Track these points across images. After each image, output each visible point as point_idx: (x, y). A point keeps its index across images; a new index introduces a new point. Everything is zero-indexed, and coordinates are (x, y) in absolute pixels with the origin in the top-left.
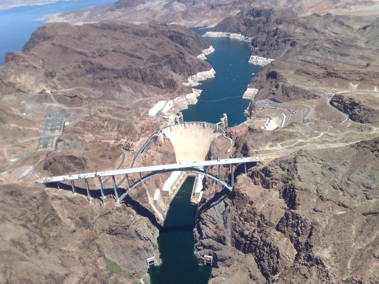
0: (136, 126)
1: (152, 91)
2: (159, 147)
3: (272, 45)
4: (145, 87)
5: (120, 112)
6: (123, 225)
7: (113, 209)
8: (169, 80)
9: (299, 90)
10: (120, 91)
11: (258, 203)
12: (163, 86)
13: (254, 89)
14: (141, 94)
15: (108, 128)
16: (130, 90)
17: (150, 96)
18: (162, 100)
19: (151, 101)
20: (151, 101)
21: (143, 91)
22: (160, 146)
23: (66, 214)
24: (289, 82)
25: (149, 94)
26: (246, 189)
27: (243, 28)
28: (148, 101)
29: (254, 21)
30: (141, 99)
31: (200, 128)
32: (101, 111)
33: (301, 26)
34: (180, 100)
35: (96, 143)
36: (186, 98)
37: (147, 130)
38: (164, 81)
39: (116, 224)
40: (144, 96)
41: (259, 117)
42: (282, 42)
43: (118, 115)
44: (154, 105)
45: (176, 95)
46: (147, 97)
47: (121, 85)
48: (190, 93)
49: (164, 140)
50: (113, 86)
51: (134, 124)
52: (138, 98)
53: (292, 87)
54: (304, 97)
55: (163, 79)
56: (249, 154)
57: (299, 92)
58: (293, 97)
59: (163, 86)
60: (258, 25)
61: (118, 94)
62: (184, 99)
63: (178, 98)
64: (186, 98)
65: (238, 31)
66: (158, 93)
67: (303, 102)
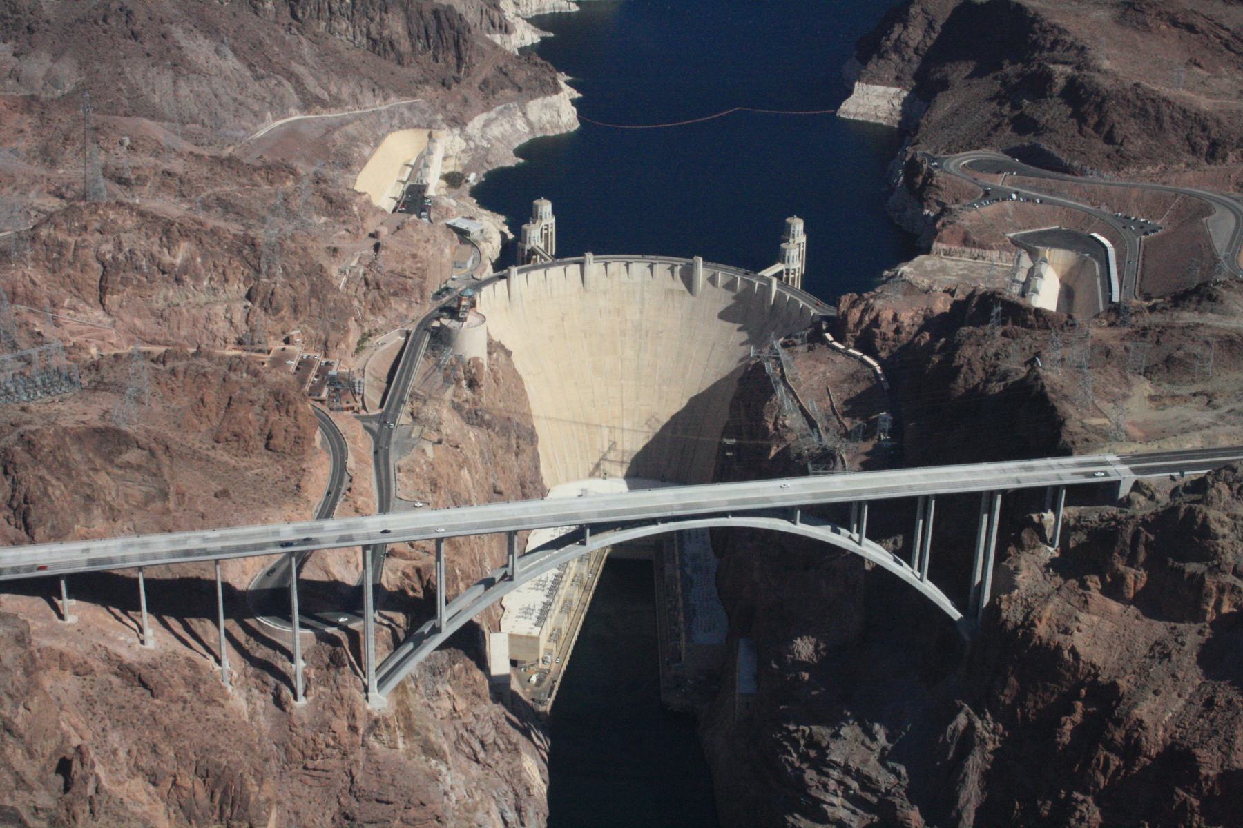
0: (334, 271)
1: (345, 70)
2: (467, 393)
4: (306, 49)
5: (228, 188)
6: (413, 813)
7: (353, 729)
8: (436, 13)
9: (1164, 107)
10: (179, 65)
11: (1151, 696)
12: (405, 46)
14: (289, 87)
15: (197, 279)
16: (231, 63)
17: (337, 102)
18: (404, 124)
19: (350, 129)
20: (350, 129)
22: (473, 384)
23: (122, 755)
24: (1106, 65)
25: (334, 90)
26: (1073, 626)
28: (330, 129)
30: (296, 116)
31: (669, 292)
32: (123, 181)
35: (181, 365)
37: (395, 294)
38: (409, 19)
39: (380, 811)
40: (308, 102)
41: (974, 245)
43: (226, 205)
44: (366, 151)
45: (476, 99)
46: (325, 105)
47: (178, 33)
48: (546, 94)
49: (490, 353)
50: (134, 36)
51: (323, 259)
52: (280, 108)
53: (1130, 95)
54: (1194, 150)
56: (1066, 438)
57: (1167, 124)
58: (1136, 145)
61: (166, 80)
63: (484, 117)
66: (379, 88)
67: (1190, 175)
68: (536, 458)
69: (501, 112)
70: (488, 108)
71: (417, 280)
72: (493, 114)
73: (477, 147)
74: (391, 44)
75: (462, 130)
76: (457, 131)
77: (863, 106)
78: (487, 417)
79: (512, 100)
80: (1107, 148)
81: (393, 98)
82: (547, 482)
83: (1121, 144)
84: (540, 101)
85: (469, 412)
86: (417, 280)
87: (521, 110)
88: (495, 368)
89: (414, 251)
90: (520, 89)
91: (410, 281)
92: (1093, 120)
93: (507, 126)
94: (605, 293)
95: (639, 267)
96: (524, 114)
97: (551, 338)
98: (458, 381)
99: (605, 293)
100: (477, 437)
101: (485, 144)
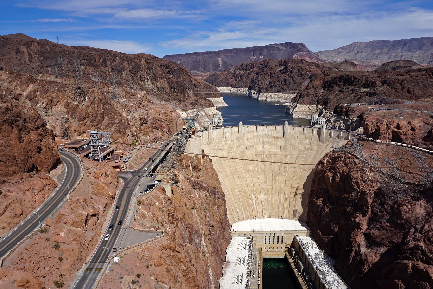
2: (192, 173)
3: (285, 81)
13: (308, 105)
22: (196, 168)
27: (232, 81)
29: (245, 74)
36: (205, 113)
38: (169, 83)
42: (298, 76)
45: (189, 106)
48: (210, 107)
59: (168, 90)
60: (251, 76)
62: (203, 113)
63: (192, 110)
64: (205, 113)
65: (228, 85)
68: (225, 209)
70: (193, 108)
71: (167, 123)
72: (195, 110)
74: (163, 89)
75: (186, 112)
76: (184, 113)
78: (204, 185)
80: (409, 95)
81: (163, 102)
82: (230, 221)
83: (414, 93)
85: (194, 182)
86: (167, 123)
88: (206, 163)
89: (165, 111)
90: (202, 106)
91: (163, 123)
92: (400, 87)
94: (248, 140)
95: (261, 128)
96: (204, 112)
98: (187, 167)
99: (248, 140)
100: (199, 195)
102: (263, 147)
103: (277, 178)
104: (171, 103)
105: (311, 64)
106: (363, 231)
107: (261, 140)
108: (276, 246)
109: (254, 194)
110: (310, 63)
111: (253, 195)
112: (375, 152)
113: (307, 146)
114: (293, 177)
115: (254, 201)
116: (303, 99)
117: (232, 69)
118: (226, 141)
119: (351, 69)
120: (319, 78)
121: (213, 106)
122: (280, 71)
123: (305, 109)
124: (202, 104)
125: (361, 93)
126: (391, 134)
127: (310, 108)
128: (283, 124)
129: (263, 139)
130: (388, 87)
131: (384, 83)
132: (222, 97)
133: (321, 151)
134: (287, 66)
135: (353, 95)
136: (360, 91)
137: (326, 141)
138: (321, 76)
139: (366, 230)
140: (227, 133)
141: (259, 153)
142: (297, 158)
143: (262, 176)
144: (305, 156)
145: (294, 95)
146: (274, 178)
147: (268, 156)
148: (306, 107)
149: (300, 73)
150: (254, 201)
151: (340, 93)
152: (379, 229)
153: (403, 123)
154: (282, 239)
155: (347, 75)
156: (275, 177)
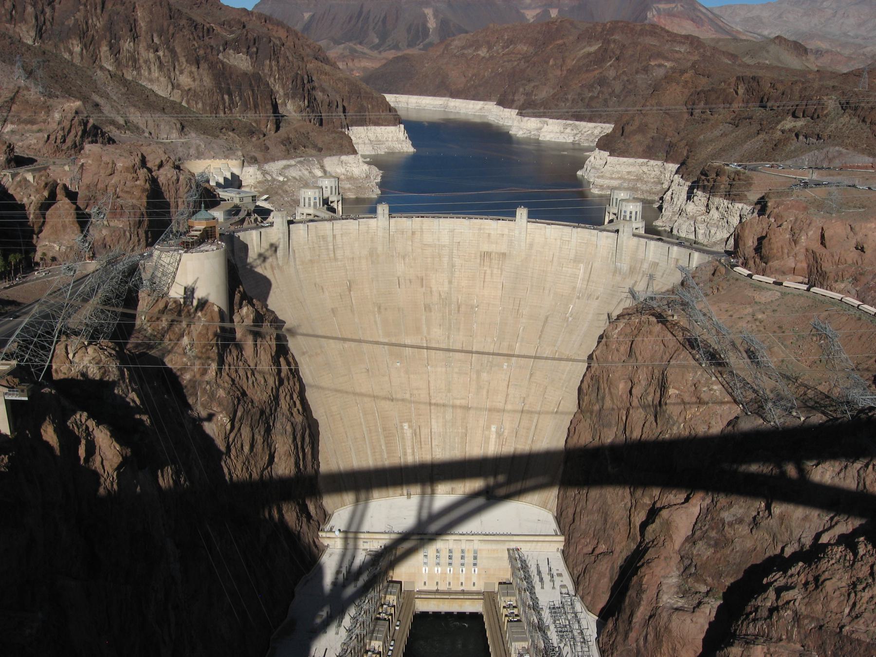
13: (642, 160)
21: (97, 98)
31: (486, 256)
33: (684, 43)
34: (293, 173)
55: (212, 66)
62: (318, 173)
69: (300, 162)
70: (287, 155)
72: (292, 162)
73: (274, 180)
77: (618, 172)
79: (311, 156)
81: (193, 135)
84: (335, 159)
87: (319, 163)
90: (320, 150)
93: (306, 173)
94: (404, 258)
96: (322, 167)
97: (333, 311)
99: (404, 258)
101: (281, 179)
102: (450, 282)
103: (484, 376)
104: (218, 141)
105: (678, 39)
106: (677, 547)
107: (446, 260)
108: (458, 579)
109: (410, 421)
110: (676, 35)
111: (406, 426)
112: (749, 310)
113: (578, 285)
114: (531, 375)
115: (409, 443)
116: (628, 141)
117: (456, 43)
118: (336, 259)
119: (793, 62)
120: (678, 84)
121: (355, 152)
122: (589, 54)
123: (629, 173)
124: (320, 145)
125: (783, 132)
126: (801, 257)
127: (645, 169)
128: (512, 215)
129: (451, 257)
130: (855, 120)
131: (845, 106)
132: (402, 126)
133: (615, 302)
134: (609, 42)
135: (760, 136)
136: (779, 127)
137: (632, 270)
138: (687, 76)
139: (683, 544)
140: (338, 237)
141: (435, 298)
142: (547, 318)
143: (439, 369)
144: (571, 315)
145: (608, 128)
146: (474, 376)
147: (463, 309)
148: (633, 165)
149: (644, 64)
150: (409, 443)
151: (730, 127)
152: (717, 545)
153: (836, 229)
154: (475, 558)
155: (754, 78)
156: (478, 373)
